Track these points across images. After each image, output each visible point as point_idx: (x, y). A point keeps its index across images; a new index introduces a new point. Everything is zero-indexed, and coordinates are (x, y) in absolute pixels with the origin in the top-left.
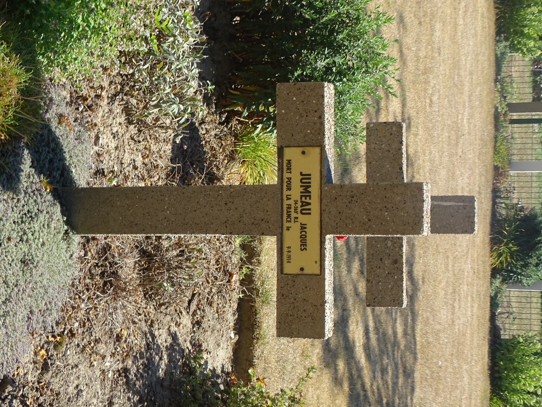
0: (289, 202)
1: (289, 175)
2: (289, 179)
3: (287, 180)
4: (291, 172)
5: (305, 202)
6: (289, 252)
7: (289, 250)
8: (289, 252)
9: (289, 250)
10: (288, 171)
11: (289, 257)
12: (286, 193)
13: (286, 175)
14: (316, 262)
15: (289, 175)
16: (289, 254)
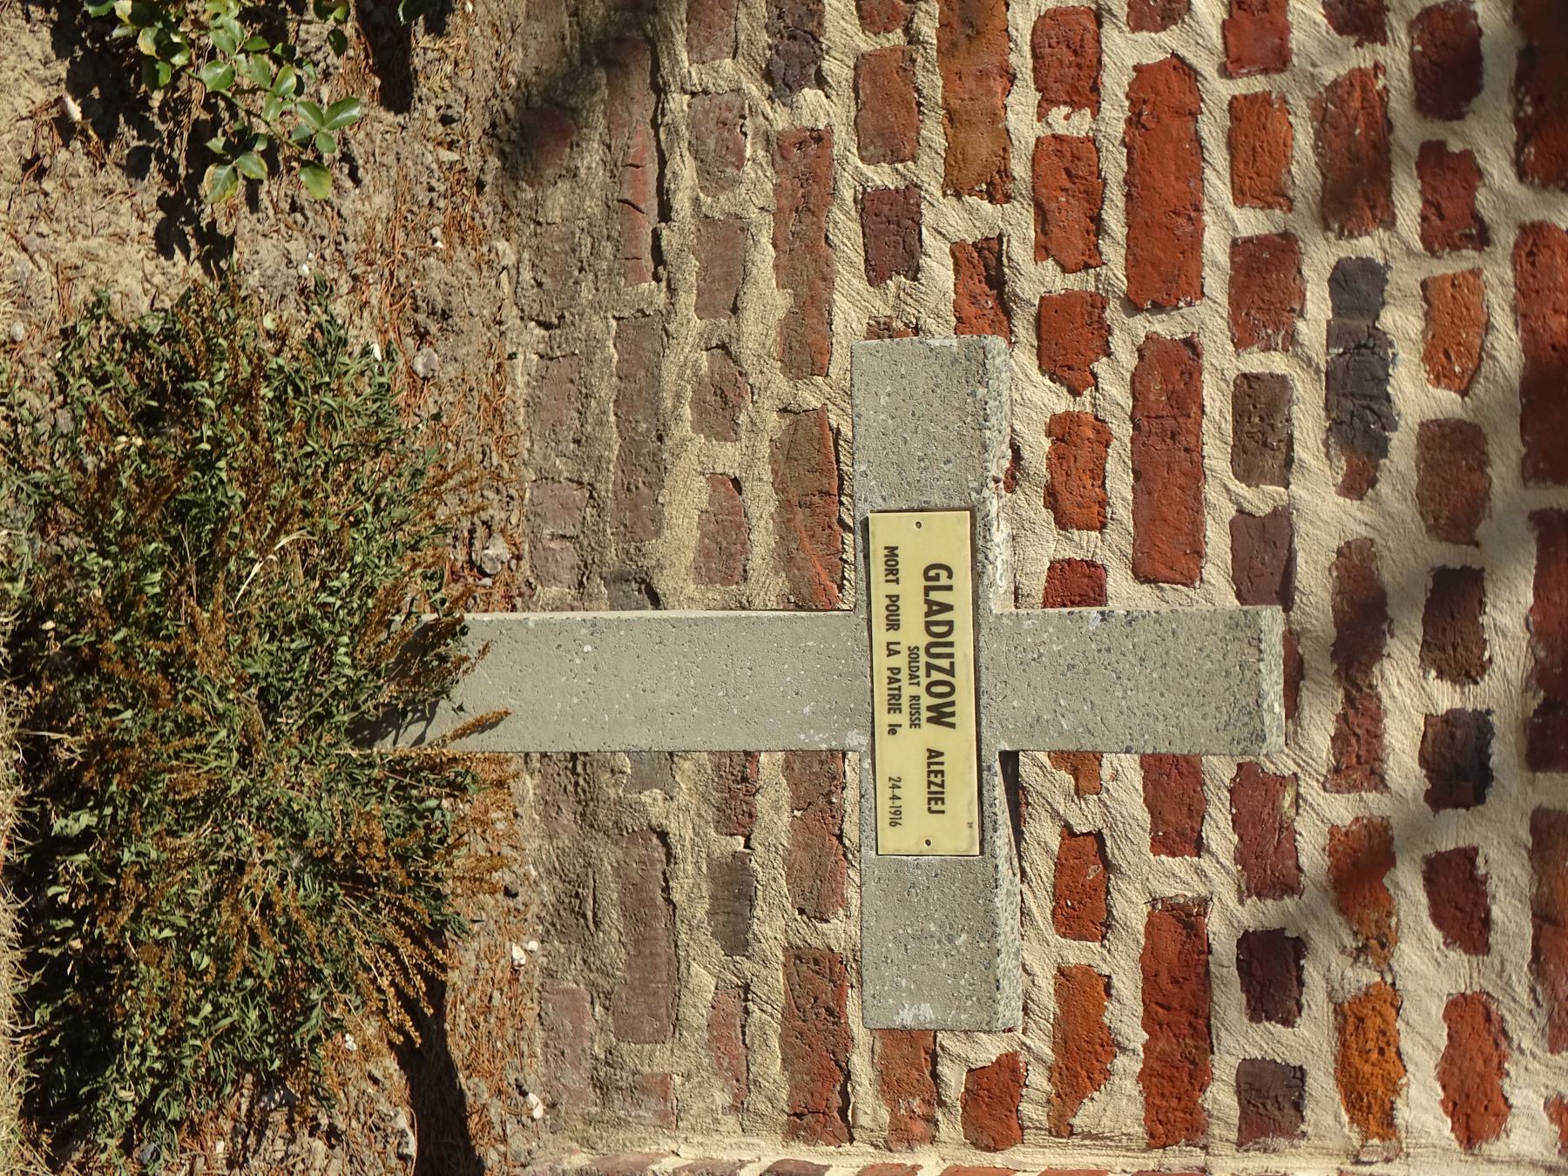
0: (895, 661)
1: (893, 589)
2: (894, 599)
3: (887, 602)
4: (897, 581)
5: (937, 603)
6: (895, 797)
7: (897, 792)
8: (895, 797)
9: (897, 792)
10: (891, 577)
11: (897, 812)
12: (881, 636)
13: (881, 589)
14: (970, 825)
15: (893, 589)
16: (897, 803)
